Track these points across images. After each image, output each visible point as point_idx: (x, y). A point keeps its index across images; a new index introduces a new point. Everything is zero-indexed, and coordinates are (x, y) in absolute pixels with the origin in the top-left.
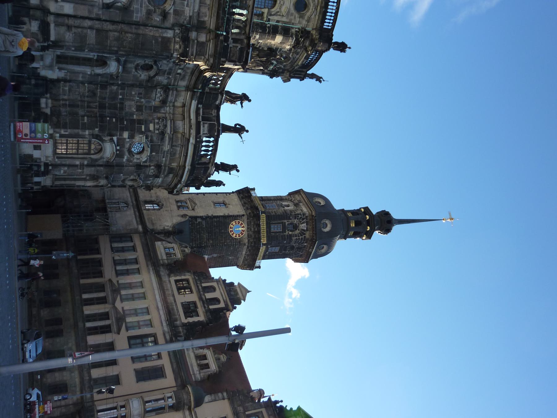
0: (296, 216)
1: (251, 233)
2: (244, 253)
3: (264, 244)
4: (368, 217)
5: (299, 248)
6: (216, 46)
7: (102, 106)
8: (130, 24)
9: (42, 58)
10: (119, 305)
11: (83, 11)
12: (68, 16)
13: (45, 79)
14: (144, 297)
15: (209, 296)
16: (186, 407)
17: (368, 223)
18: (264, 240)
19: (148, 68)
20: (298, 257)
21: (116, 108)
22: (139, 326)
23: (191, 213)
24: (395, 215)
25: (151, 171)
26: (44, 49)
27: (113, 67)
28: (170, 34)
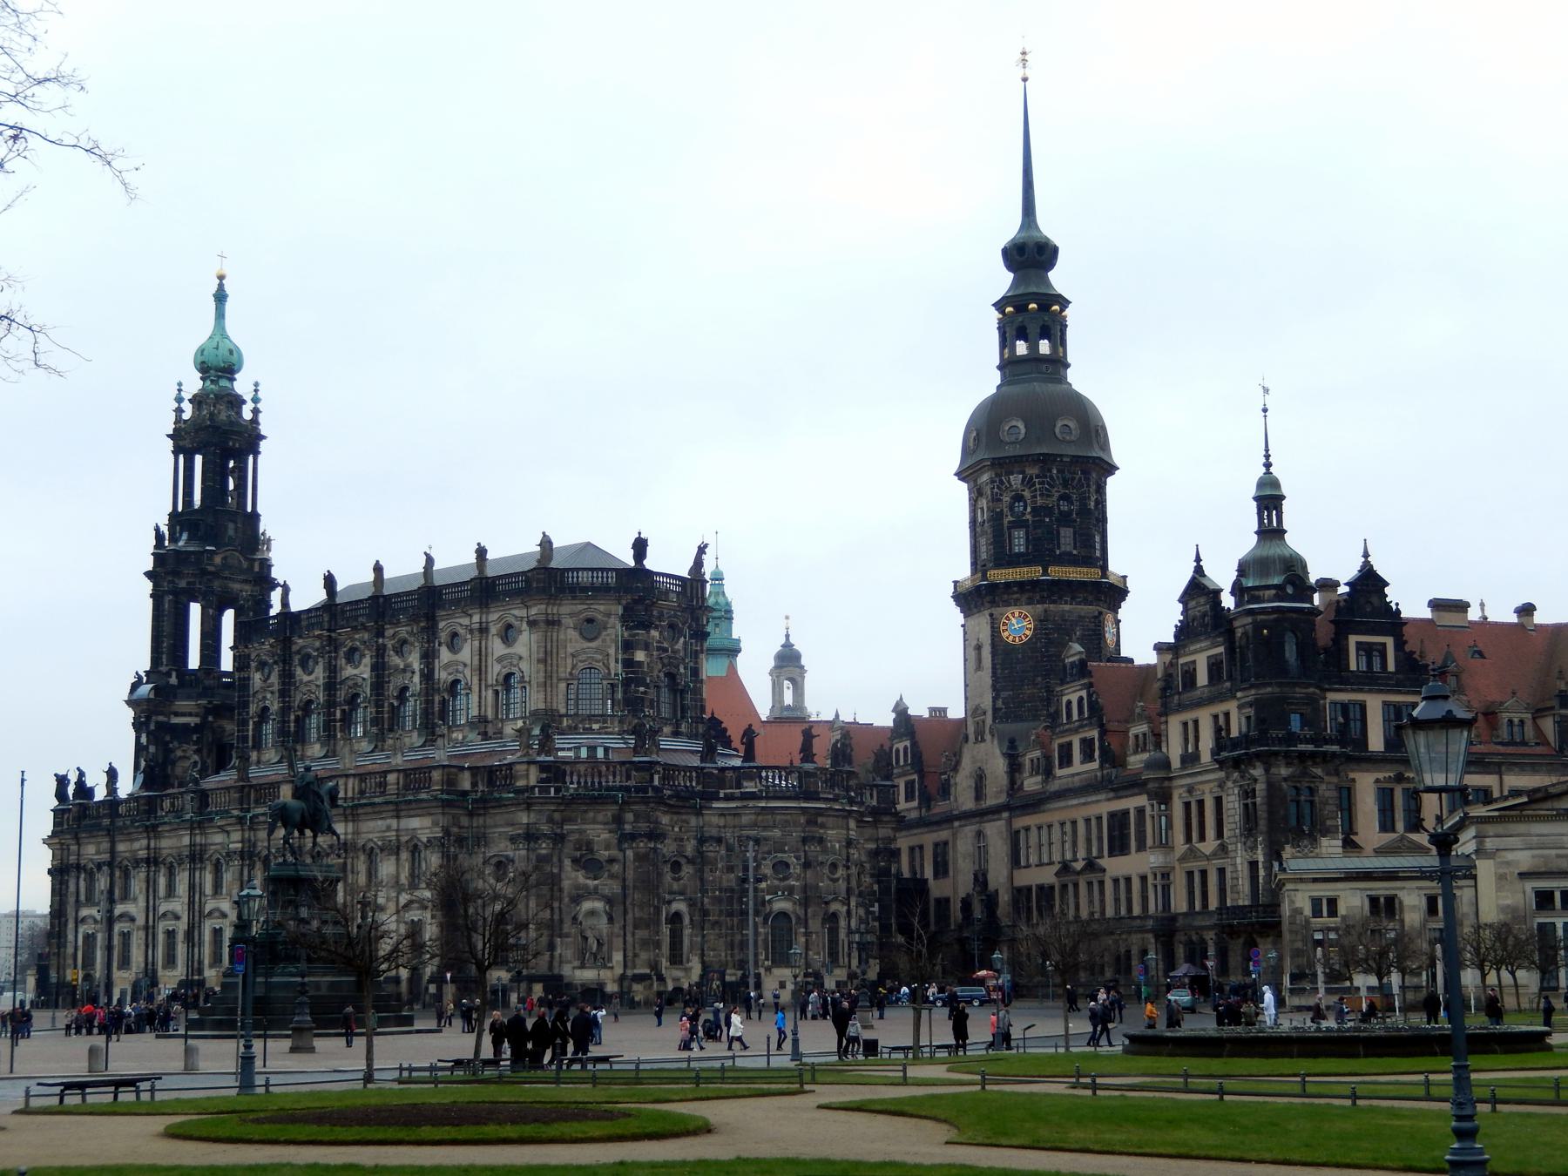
0: (996, 499)
1: (1024, 598)
2: (1067, 607)
3: (1045, 573)
4: (1009, 309)
5: (1065, 484)
6: (635, 803)
7: (730, 914)
8: (625, 896)
9: (676, 980)
10: (1079, 866)
11: (618, 942)
12: (625, 956)
13: (702, 977)
14: (1074, 823)
15: (1075, 716)
16: (1166, 784)
17: (1021, 308)
18: (1033, 572)
19: (676, 867)
20: (1088, 479)
21: (731, 898)
22: (1100, 839)
23: (989, 720)
24: (1009, 228)
25: (813, 849)
26: (661, 979)
27: (680, 906)
28: (630, 853)
